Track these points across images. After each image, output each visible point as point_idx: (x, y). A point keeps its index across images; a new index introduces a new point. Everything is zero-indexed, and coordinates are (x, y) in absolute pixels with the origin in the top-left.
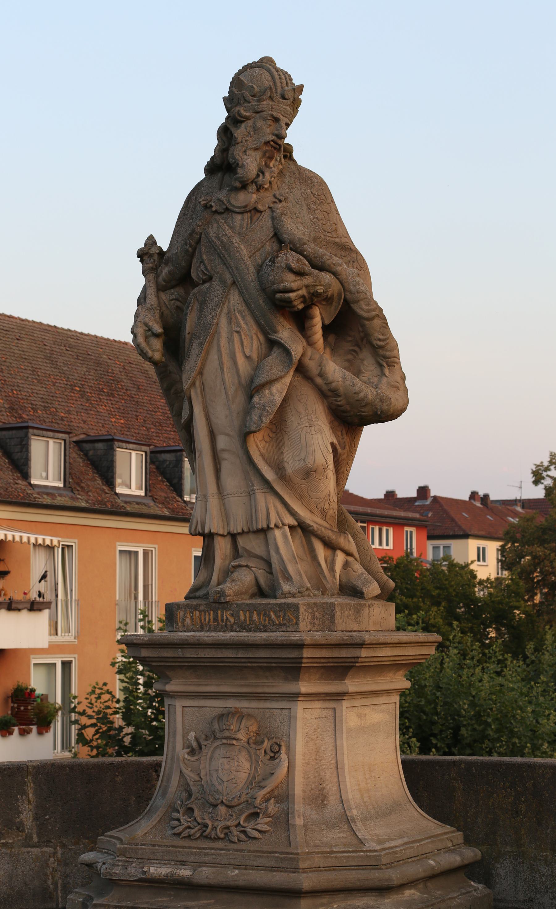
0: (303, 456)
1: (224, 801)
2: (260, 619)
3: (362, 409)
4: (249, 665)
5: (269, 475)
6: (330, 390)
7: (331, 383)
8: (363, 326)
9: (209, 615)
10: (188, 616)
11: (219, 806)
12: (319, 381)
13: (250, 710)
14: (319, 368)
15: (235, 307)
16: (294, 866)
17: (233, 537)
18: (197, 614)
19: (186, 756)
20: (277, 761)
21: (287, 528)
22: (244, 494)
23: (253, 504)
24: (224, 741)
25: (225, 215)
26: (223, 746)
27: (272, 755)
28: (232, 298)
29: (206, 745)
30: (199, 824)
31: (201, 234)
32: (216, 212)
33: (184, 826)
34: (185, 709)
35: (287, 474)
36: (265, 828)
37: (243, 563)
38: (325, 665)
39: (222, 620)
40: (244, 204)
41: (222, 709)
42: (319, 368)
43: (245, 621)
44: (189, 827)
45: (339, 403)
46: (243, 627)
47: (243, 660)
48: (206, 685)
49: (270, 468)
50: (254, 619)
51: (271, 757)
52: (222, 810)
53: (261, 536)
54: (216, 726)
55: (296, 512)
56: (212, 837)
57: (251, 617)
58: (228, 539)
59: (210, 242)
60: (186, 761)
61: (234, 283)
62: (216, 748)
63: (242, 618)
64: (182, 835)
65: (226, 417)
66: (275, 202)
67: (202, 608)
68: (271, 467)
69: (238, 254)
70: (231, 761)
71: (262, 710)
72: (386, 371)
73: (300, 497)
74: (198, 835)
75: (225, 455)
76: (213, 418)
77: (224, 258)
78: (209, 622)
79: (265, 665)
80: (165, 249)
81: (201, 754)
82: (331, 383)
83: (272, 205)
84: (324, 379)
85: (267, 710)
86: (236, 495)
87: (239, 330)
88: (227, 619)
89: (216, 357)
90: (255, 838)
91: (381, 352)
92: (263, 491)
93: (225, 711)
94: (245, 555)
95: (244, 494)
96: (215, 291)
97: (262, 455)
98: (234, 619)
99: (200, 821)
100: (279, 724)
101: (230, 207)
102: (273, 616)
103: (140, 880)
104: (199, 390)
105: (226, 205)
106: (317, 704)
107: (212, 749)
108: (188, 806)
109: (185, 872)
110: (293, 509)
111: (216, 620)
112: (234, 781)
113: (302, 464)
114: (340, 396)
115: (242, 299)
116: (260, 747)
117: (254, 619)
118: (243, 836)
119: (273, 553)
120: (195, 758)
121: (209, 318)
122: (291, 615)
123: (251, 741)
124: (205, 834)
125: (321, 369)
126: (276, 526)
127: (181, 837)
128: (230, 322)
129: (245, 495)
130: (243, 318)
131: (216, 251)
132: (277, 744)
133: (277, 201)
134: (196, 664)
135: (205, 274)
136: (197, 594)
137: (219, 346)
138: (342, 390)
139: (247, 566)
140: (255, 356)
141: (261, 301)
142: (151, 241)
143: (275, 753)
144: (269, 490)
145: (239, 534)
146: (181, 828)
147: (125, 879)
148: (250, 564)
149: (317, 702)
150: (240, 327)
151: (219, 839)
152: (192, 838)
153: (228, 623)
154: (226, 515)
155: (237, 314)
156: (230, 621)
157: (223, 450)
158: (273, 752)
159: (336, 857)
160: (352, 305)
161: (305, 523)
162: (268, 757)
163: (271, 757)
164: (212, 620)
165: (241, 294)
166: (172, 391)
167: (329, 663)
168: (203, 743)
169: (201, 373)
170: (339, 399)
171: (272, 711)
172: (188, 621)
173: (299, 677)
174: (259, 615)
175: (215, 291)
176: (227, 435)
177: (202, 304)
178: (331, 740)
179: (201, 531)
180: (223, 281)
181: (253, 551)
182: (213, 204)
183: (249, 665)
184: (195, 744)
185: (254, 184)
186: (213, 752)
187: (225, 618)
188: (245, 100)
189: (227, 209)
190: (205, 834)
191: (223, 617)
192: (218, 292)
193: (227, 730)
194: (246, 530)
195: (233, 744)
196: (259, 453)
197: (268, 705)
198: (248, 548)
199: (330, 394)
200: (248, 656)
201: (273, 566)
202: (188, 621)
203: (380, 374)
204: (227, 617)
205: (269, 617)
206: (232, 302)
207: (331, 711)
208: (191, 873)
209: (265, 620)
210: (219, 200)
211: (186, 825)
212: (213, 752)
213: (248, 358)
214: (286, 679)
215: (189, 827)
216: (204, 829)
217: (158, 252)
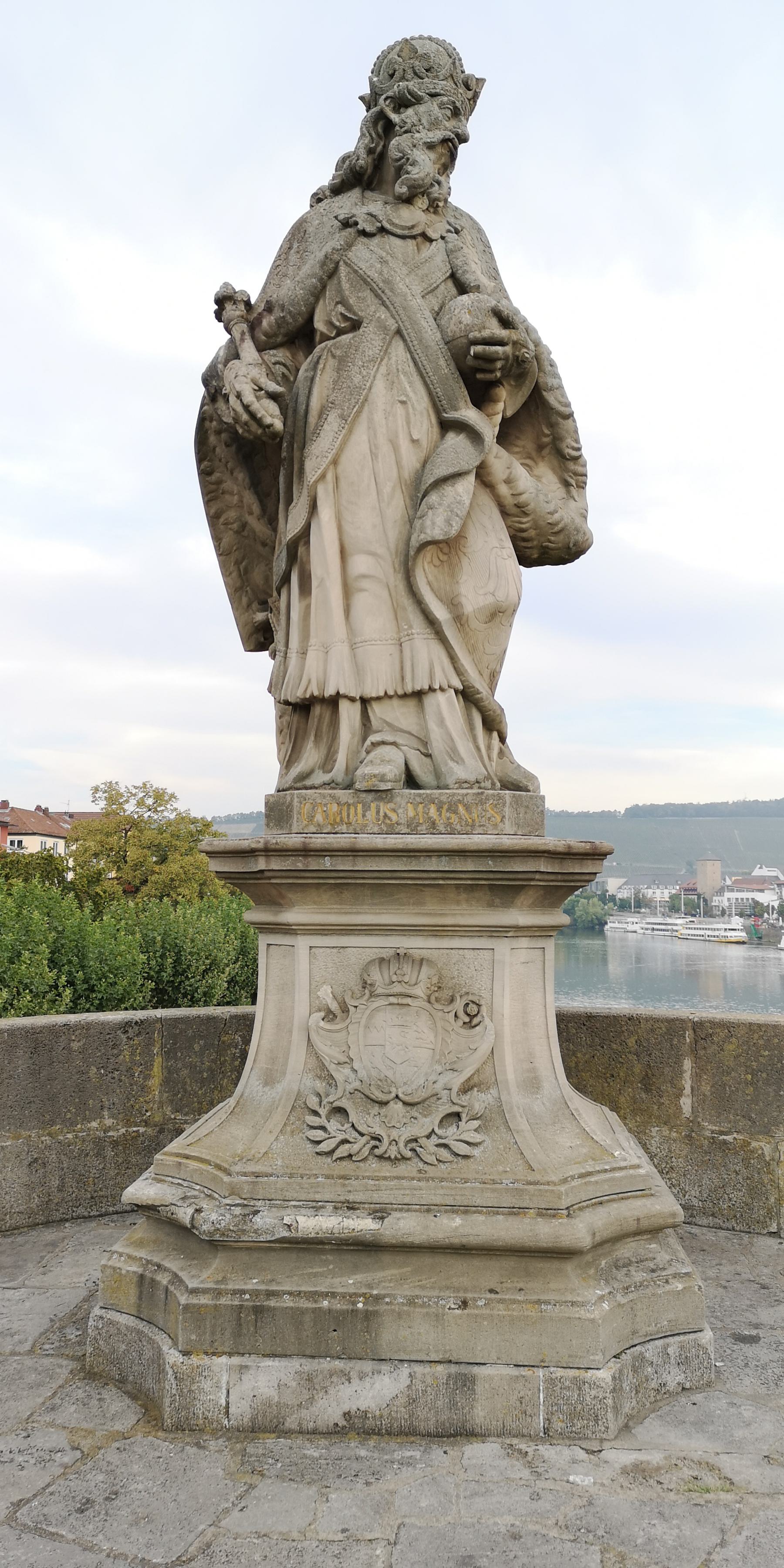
0: (491, 587)
1: (401, 1095)
3: (552, 538)
4: (441, 882)
5: (440, 612)
6: (517, 506)
7: (520, 494)
8: (552, 426)
10: (320, 810)
11: (392, 1103)
12: (503, 490)
17: (365, 702)
19: (322, 1024)
21: (452, 691)
22: (390, 642)
24: (393, 1000)
25: (376, 240)
26: (390, 1007)
27: (467, 1019)
28: (393, 354)
29: (356, 1007)
30: (362, 1135)
31: (338, 263)
33: (338, 1140)
35: (466, 613)
36: (476, 1138)
37: (389, 738)
38: (551, 884)
40: (409, 224)
41: (376, 950)
42: (508, 471)
45: (523, 526)
47: (434, 875)
48: (358, 913)
49: (440, 604)
51: (464, 1023)
52: (397, 1108)
53: (412, 703)
54: (376, 976)
55: (466, 671)
56: (393, 1157)
58: (358, 705)
60: (322, 1032)
62: (377, 1009)
68: (442, 601)
71: (445, 951)
72: (574, 491)
73: (472, 650)
74: (366, 1152)
75: (365, 584)
76: (347, 528)
79: (469, 882)
80: (253, 301)
81: (348, 1021)
82: (520, 494)
83: (445, 234)
84: (511, 488)
86: (379, 642)
87: (405, 399)
88: (386, 816)
89: (365, 437)
90: (466, 1157)
91: (571, 466)
93: (385, 954)
94: (386, 728)
95: (390, 642)
97: (429, 584)
101: (387, 226)
104: (330, 486)
106: (524, 942)
107: (368, 1012)
108: (335, 1105)
110: (463, 665)
113: (490, 599)
114: (526, 514)
115: (409, 356)
116: (450, 1008)
118: (444, 1154)
119: (433, 726)
121: (357, 379)
123: (433, 999)
124: (377, 1152)
125: (511, 473)
126: (442, 689)
128: (391, 385)
129: (393, 642)
132: (473, 1002)
133: (453, 230)
134: (350, 881)
135: (345, 318)
136: (308, 782)
137: (371, 421)
138: (531, 506)
139: (394, 744)
140: (424, 443)
143: (472, 1017)
144: (433, 636)
145: (378, 699)
148: (400, 741)
149: (524, 939)
151: (404, 1158)
152: (354, 1158)
154: (358, 670)
155: (402, 376)
156: (389, 818)
157: (364, 576)
158: (468, 1015)
159: (597, 1182)
160: (545, 393)
161: (474, 687)
162: (460, 1023)
163: (464, 1023)
166: (222, 520)
168: (351, 1002)
169: (335, 462)
170: (524, 520)
173: (512, 902)
174: (439, 809)
176: (373, 554)
177: (342, 363)
179: (316, 693)
181: (396, 724)
183: (441, 882)
184: (334, 1006)
185: (425, 197)
186: (371, 1017)
189: (382, 230)
190: (377, 1152)
192: (373, 342)
193: (400, 982)
195: (409, 1005)
196: (425, 580)
198: (388, 720)
199: (514, 510)
201: (435, 744)
203: (565, 496)
206: (394, 359)
210: (370, 214)
211: (341, 1137)
214: (491, 905)
216: (373, 1143)
217: (245, 299)
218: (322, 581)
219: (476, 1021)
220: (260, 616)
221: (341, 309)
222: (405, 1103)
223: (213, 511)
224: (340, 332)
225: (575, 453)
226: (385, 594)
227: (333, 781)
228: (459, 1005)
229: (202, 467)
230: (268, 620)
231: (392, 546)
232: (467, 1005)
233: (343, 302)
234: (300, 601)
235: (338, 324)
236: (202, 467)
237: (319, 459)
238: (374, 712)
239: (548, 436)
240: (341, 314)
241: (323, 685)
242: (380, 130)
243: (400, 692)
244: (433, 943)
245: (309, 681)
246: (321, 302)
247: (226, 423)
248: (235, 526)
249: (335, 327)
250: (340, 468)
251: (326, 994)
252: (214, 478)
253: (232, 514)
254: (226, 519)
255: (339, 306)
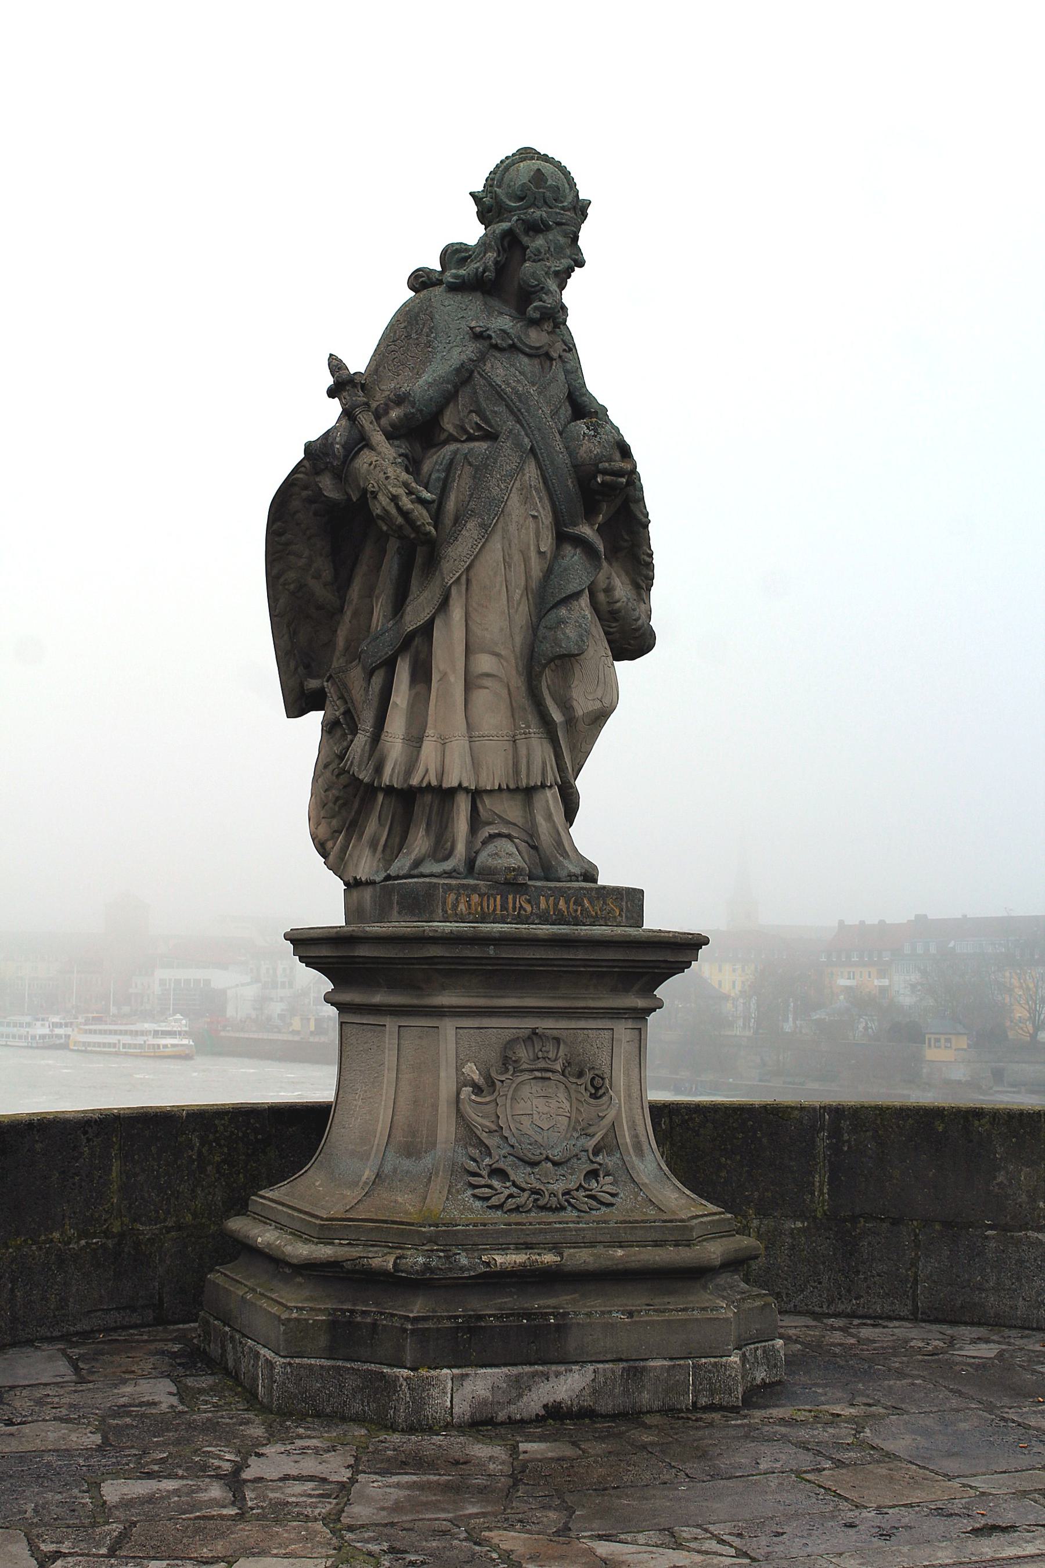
2: (568, 908)
9: (495, 901)
13: (555, 1031)
14: (607, 581)
15: (532, 483)
16: (685, 1238)
17: (476, 795)
18: (475, 898)
20: (605, 1099)
23: (523, 751)
24: (538, 1074)
28: (527, 470)
29: (502, 1081)
30: (523, 1190)
32: (495, 347)
34: (461, 1031)
39: (514, 910)
40: (538, 345)
41: (514, 1031)
42: (607, 581)
43: (547, 911)
44: (511, 1196)
45: (611, 630)
46: (545, 919)
50: (560, 907)
53: (519, 797)
54: (523, 1053)
57: (556, 904)
59: (490, 385)
61: (532, 450)
63: (543, 905)
64: (507, 1207)
65: (501, 630)
66: (564, 350)
67: (484, 890)
69: (540, 411)
70: (550, 1101)
71: (572, 1031)
73: (573, 749)
76: (473, 627)
77: (519, 413)
78: (495, 910)
84: (608, 597)
85: (579, 1031)
87: (536, 514)
88: (521, 907)
92: (539, 736)
95: (506, 738)
96: (505, 456)
98: (532, 907)
99: (524, 1185)
100: (596, 1050)
101: (519, 344)
102: (587, 904)
103: (484, 1275)
104: (464, 587)
105: (512, 340)
107: (514, 1085)
109: (549, 1258)
111: (504, 907)
112: (556, 1129)
114: (616, 620)
117: (560, 907)
119: (540, 820)
120: (488, 1099)
122: (612, 903)
124: (540, 1203)
125: (610, 583)
127: (505, 1209)
130: (540, 498)
131: (504, 399)
135: (479, 427)
139: (509, 837)
141: (569, 483)
142: (335, 365)
143: (597, 1089)
146: (502, 1197)
147: (456, 1275)
150: (538, 511)
152: (521, 1209)
153: (522, 912)
154: (476, 764)
156: (525, 911)
157: (488, 675)
160: (631, 505)
164: (499, 907)
165: (539, 466)
166: (282, 580)
167: (625, 967)
171: (585, 1032)
172: (462, 907)
174: (567, 902)
175: (505, 456)
176: (497, 655)
178: (637, 1070)
179: (434, 783)
180: (518, 445)
182: (493, 335)
186: (516, 1090)
187: (518, 905)
188: (545, 202)
191: (514, 903)
194: (512, 786)
195: (550, 1079)
197: (582, 1024)
200: (592, 957)
202: (462, 907)
204: (520, 904)
205: (583, 906)
207: (637, 1032)
208: (559, 1259)
209: (576, 911)
211: (507, 1192)
212: (516, 1090)
213: (541, 553)
215: (511, 1196)
218: (444, 676)
219: (601, 1092)
220: (313, 684)
221: (476, 419)
222: (555, 1164)
223: (275, 572)
224: (471, 438)
225: (648, 559)
226: (504, 692)
227: (455, 871)
228: (588, 1076)
229: (275, 527)
230: (323, 688)
231: (518, 649)
232: (593, 1079)
233: (479, 412)
234: (410, 690)
235: (472, 431)
236: (275, 527)
237: (456, 562)
238: (483, 802)
239: (626, 541)
240: (476, 423)
241: (441, 774)
242: (506, 244)
243: (512, 786)
244: (563, 1024)
245: (427, 771)
246: (452, 405)
247: (325, 496)
248: (292, 587)
249: (466, 432)
250: (472, 573)
251: (472, 1071)
252: (283, 539)
253: (292, 575)
254: (286, 580)
255: (474, 414)
